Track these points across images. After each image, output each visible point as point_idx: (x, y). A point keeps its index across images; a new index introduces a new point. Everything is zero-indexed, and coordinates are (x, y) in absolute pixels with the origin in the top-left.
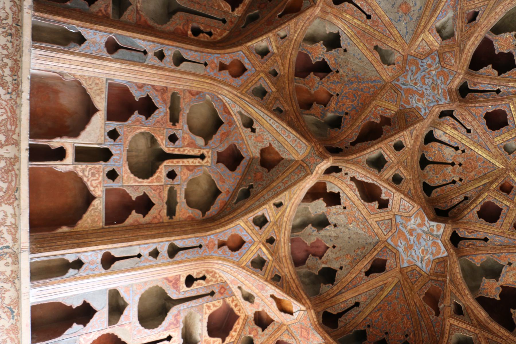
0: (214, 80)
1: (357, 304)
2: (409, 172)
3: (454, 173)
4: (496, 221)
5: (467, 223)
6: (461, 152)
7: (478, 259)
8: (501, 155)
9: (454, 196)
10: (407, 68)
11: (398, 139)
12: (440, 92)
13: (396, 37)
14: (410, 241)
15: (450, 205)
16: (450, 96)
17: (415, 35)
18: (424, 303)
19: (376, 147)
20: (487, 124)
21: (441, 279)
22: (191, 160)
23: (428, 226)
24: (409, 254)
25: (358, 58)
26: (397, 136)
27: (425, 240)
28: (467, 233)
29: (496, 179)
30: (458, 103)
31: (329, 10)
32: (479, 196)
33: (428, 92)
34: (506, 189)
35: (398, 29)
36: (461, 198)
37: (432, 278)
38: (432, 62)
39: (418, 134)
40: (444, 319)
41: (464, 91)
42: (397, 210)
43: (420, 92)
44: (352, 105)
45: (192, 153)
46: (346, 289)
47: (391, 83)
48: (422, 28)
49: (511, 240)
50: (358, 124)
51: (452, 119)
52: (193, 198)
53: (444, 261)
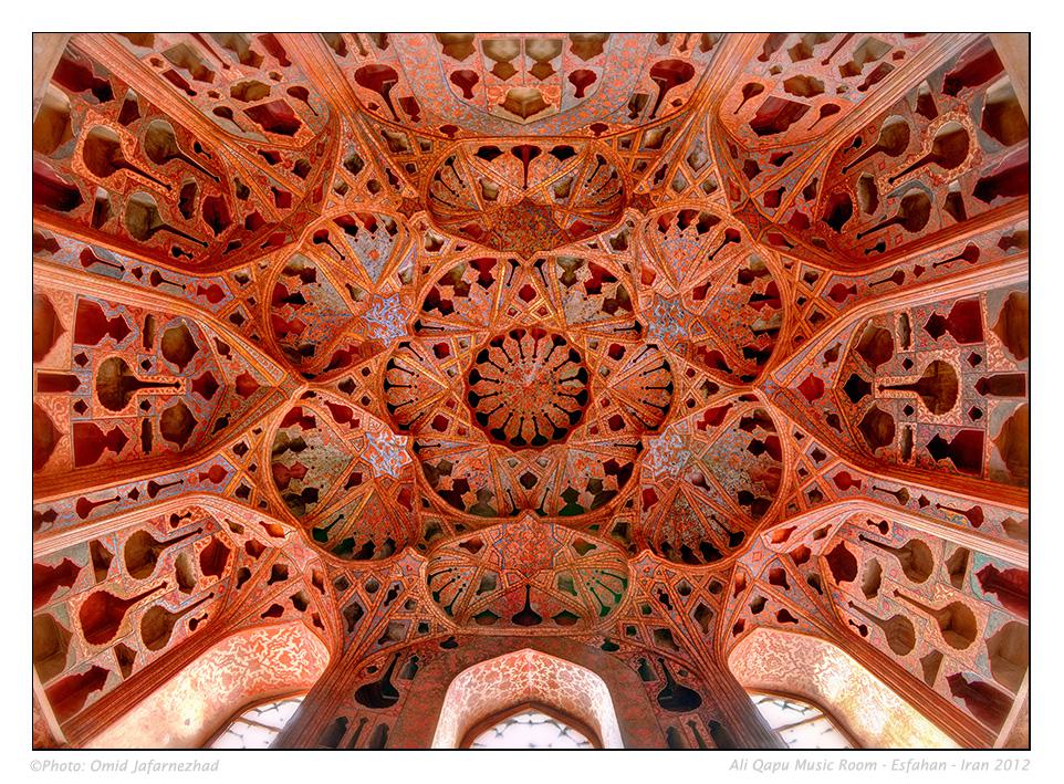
0: (191, 304)
1: (341, 517)
7: (435, 462)
22: (165, 389)
31: (309, 247)
34: (450, 404)
36: (417, 415)
41: (418, 326)
45: (167, 381)
46: (330, 504)
52: (170, 431)
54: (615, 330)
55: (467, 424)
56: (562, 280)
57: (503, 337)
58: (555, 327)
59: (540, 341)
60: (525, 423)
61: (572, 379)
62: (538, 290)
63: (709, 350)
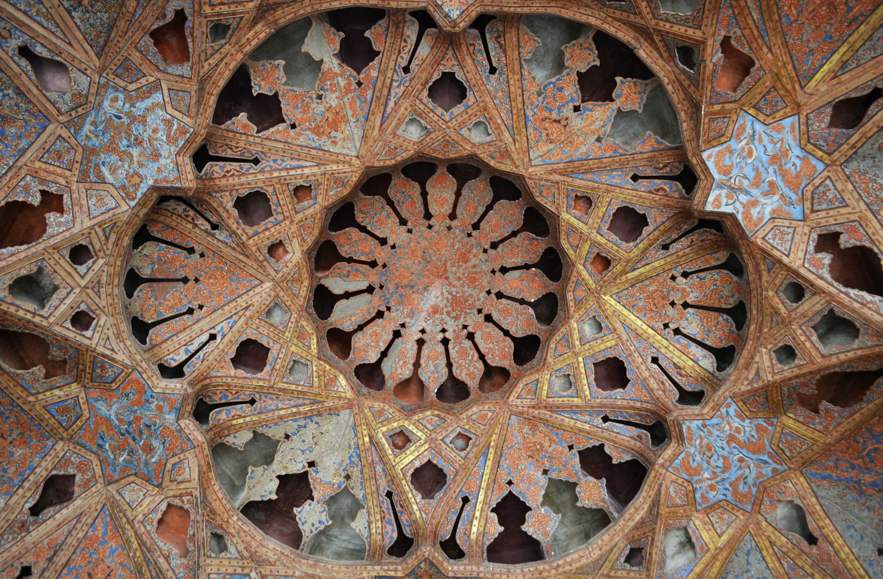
2: (769, 304)
3: (684, 290)
4: (619, 209)
5: (666, 206)
6: (670, 325)
8: (607, 317)
9: (687, 251)
10: (754, 490)
11: (786, 368)
12: (698, 442)
13: (770, 550)
14: (775, 172)
15: (695, 236)
16: (681, 431)
17: (733, 546)
18: (753, 56)
19: (834, 360)
20: (624, 370)
21: (717, 108)
23: (738, 205)
24: (779, 145)
25: (853, 530)
26: (787, 374)
27: (745, 177)
28: (666, 188)
29: (615, 279)
30: (669, 418)
32: (644, 251)
33: (719, 443)
34: (604, 262)
35: (763, 566)
37: (733, 105)
38: (707, 492)
39: (746, 373)
40: (714, 34)
41: (659, 431)
42: (799, 230)
43: (734, 445)
44: (879, 442)
47: (790, 469)
48: (720, 557)
49: (597, 179)
50: (870, 406)
51: (681, 384)
53: (709, 142)
54: (252, 402)
55: (569, 217)
56: (358, 505)
57: (481, 386)
58: (377, 405)
59: (407, 373)
60: (447, 209)
61: (347, 295)
62: (407, 486)
63: (39, 370)
